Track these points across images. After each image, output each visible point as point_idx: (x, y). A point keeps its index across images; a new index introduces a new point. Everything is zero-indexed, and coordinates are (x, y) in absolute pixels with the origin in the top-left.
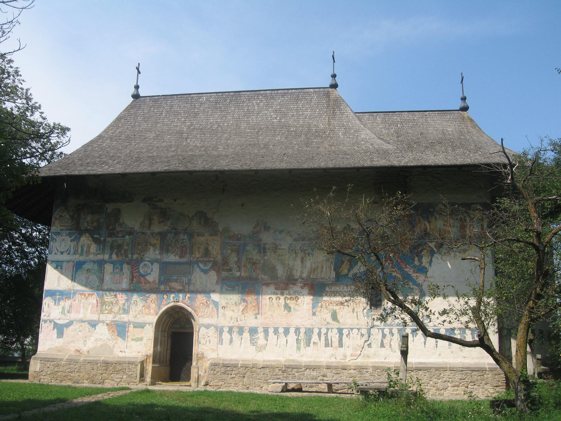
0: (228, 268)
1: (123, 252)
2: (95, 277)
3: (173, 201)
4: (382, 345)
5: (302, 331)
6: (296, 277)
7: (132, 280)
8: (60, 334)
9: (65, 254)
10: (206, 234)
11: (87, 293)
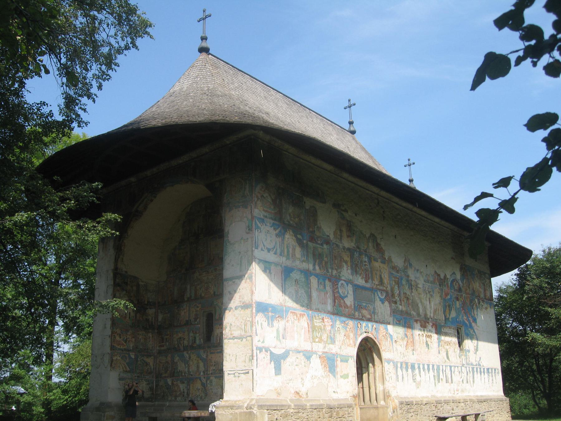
2: (303, 291)
3: (354, 215)
4: (467, 382)
5: (435, 367)
6: (429, 316)
8: (278, 370)
9: (272, 253)
10: (379, 260)
11: (298, 312)
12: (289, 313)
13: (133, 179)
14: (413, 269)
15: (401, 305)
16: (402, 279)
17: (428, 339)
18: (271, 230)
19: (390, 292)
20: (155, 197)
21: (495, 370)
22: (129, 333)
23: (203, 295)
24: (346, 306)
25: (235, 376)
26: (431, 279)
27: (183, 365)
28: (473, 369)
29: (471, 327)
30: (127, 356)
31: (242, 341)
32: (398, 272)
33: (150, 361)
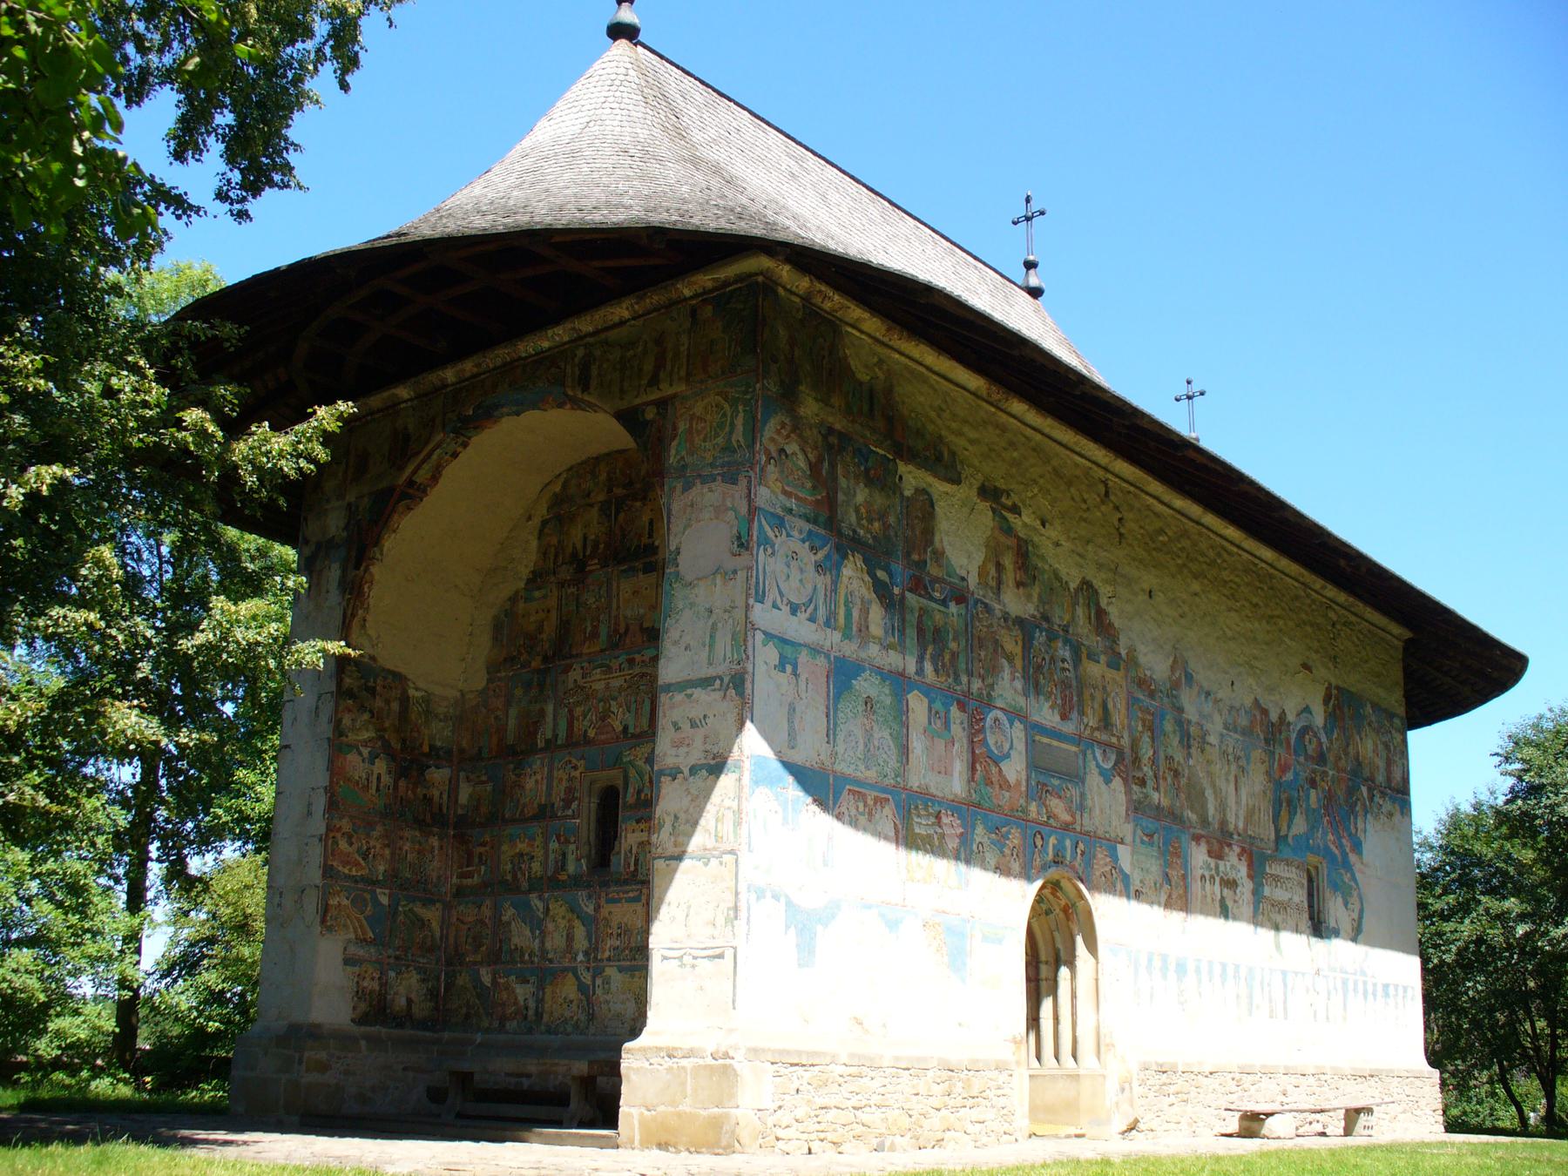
0: (1140, 775)
1: (947, 657)
2: (886, 734)
6: (1231, 827)
7: (973, 769)
8: (806, 951)
9: (802, 616)
10: (1103, 658)
12: (845, 792)
13: (403, 392)
14: (1196, 689)
15: (1157, 789)
16: (1162, 718)
17: (1225, 891)
18: (803, 549)
19: (1127, 751)
20: (465, 445)
21: (1405, 989)
22: (375, 834)
23: (591, 733)
24: (1005, 785)
25: (682, 965)
26: (1243, 721)
27: (528, 933)
28: (1344, 983)
29: (1347, 866)
30: (368, 896)
31: (706, 864)
32: (1152, 695)
33: (432, 915)
